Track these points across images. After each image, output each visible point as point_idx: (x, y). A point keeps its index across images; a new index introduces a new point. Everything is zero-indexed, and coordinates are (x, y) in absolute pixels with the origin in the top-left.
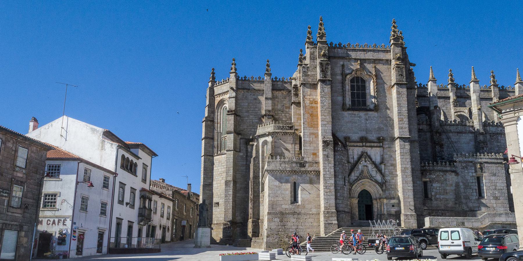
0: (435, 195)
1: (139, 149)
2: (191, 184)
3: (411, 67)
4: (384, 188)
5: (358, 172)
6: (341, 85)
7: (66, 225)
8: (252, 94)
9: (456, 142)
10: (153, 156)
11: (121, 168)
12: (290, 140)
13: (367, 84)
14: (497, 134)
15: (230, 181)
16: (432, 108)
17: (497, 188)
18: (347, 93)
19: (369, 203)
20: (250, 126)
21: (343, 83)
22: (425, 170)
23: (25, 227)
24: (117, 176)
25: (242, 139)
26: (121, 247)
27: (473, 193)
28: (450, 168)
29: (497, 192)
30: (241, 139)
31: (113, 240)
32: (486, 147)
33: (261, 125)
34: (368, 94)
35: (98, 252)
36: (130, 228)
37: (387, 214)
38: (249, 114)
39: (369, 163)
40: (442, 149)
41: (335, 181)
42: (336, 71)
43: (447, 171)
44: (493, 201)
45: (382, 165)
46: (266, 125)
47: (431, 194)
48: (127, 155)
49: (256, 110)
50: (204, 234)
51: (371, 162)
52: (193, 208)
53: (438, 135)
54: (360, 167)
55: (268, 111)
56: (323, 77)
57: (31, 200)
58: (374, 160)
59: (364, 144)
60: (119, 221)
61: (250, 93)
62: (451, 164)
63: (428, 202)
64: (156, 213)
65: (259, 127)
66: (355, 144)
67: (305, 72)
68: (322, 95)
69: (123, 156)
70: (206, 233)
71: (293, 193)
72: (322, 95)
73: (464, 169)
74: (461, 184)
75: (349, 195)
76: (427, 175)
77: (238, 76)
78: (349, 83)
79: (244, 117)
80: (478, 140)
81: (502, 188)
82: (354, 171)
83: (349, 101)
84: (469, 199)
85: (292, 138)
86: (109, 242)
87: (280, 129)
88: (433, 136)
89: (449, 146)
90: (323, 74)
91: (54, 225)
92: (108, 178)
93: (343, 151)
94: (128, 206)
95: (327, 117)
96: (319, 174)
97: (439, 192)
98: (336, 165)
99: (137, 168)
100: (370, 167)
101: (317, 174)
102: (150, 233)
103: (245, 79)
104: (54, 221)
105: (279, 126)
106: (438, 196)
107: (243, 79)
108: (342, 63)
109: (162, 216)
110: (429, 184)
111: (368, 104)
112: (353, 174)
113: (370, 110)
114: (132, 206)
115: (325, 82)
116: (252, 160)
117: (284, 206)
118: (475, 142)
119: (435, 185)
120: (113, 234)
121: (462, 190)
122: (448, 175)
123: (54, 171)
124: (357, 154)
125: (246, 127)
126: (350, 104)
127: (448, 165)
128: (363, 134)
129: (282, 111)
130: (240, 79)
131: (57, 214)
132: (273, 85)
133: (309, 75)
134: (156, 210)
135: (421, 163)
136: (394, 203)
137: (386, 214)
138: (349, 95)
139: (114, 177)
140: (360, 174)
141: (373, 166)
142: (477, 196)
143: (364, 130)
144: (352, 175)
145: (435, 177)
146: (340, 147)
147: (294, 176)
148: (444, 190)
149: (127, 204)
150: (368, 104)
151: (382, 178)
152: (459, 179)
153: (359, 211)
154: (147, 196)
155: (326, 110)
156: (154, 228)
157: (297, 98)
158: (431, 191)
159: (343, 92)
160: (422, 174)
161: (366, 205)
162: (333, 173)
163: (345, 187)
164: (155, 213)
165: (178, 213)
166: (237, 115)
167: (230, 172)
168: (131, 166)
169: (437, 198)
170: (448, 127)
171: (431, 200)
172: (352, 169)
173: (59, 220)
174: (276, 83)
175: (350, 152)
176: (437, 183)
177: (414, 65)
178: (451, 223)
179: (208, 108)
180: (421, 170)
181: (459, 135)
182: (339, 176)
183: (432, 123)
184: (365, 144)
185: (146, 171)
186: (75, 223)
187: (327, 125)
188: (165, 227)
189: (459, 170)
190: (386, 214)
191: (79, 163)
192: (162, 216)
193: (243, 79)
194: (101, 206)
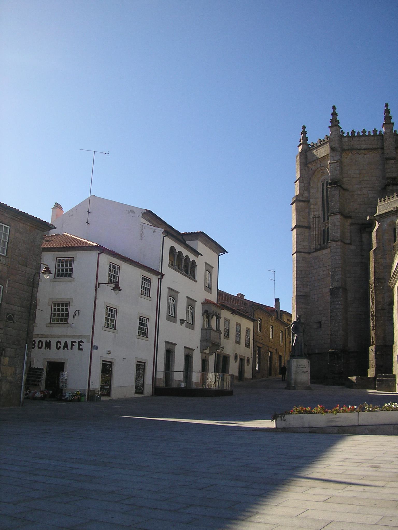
1: (198, 241)
2: (279, 299)
7: (82, 349)
10: (220, 254)
11: (169, 266)
15: (337, 288)
23: (9, 349)
24: (163, 278)
25: (353, 224)
26: (174, 385)
30: (352, 224)
31: (161, 376)
33: (383, 199)
35: (136, 393)
36: (188, 358)
38: (362, 187)
46: (391, 198)
48: (179, 248)
49: (373, 179)
50: (300, 369)
52: (284, 332)
57: (18, 308)
60: (170, 346)
61: (362, 155)
64: (229, 337)
65: (381, 201)
69: (172, 249)
70: (303, 366)
77: (342, 131)
86: (154, 379)
91: (66, 349)
92: (150, 280)
94: (184, 325)
99: (195, 269)
102: (221, 366)
103: (353, 135)
104: (66, 342)
107: (350, 135)
109: (238, 342)
114: (191, 325)
116: (372, 253)
120: (161, 365)
123: (64, 268)
130: (345, 135)
131: (69, 331)
134: (228, 333)
139: (159, 279)
149: (182, 321)
154: (213, 311)
156: (226, 359)
164: (227, 336)
165: (262, 339)
166: (344, 189)
167: (336, 274)
168: (186, 266)
173: (72, 342)
179: (299, 182)
185: (210, 274)
186: (96, 348)
188: (242, 358)
191: (99, 254)
192: (238, 342)
193: (350, 135)
194: (140, 323)
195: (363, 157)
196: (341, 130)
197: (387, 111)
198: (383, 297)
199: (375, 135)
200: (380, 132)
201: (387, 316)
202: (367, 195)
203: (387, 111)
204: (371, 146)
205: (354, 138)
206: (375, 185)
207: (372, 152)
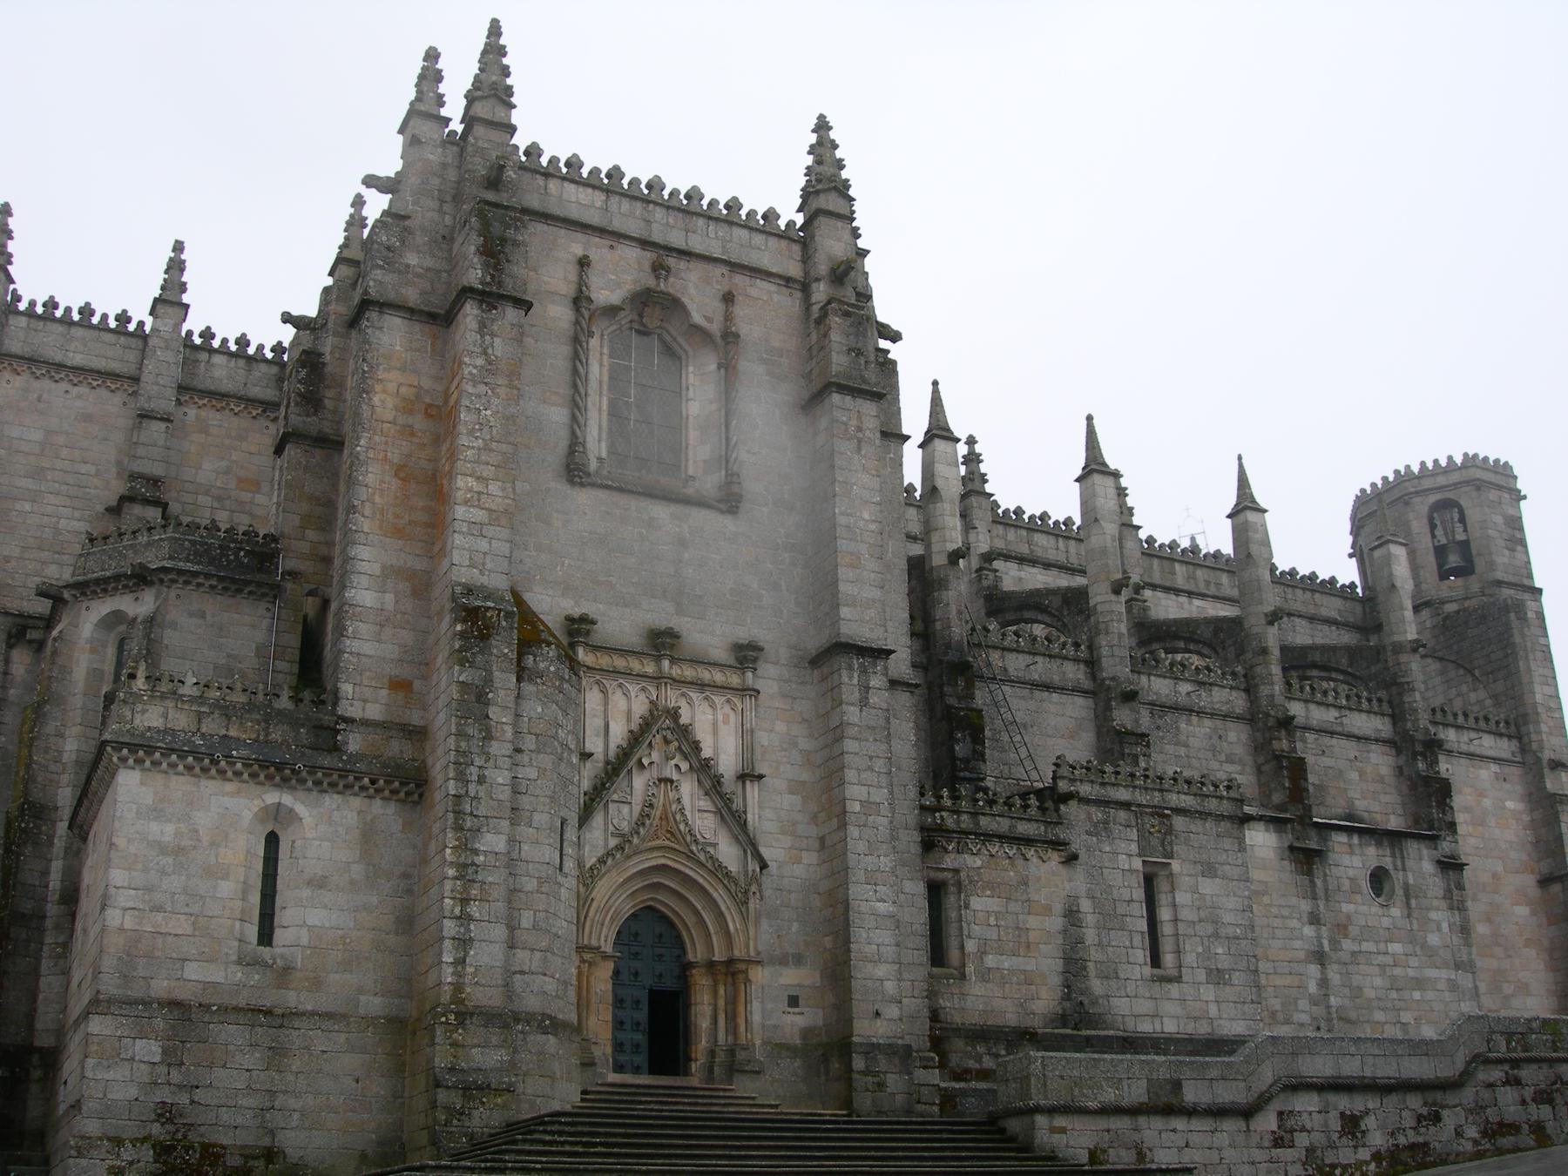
0: (982, 953)
3: (883, 344)
4: (753, 904)
5: (625, 809)
6: (565, 350)
8: (75, 391)
9: (1025, 726)
12: (254, 627)
13: (691, 376)
14: (1176, 708)
16: (938, 560)
17: (1223, 932)
18: (592, 399)
19: (670, 984)
20: (40, 549)
21: (576, 340)
22: (941, 829)
27: (1130, 950)
28: (1043, 828)
29: (1220, 951)
32: (1144, 756)
34: (691, 420)
37: (765, 1043)
38: (43, 488)
39: (684, 766)
40: (979, 748)
41: (512, 841)
42: (546, 279)
43: (1028, 841)
44: (1208, 993)
45: (748, 782)
47: (962, 948)
51: (696, 764)
53: (961, 683)
54: (639, 782)
55: (148, 480)
56: (488, 279)
58: (707, 752)
59: (666, 663)
61: (64, 386)
62: (1046, 805)
63: (949, 985)
66: (620, 663)
67: (388, 248)
68: (475, 371)
71: (255, 898)
72: (475, 371)
73: (1096, 835)
74: (1085, 905)
75: (575, 928)
76: (946, 850)
78: (601, 354)
79: (16, 499)
80: (1115, 723)
81: (1238, 931)
82: (606, 806)
83: (599, 441)
84: (1117, 978)
85: (269, 615)
87: (205, 559)
88: (941, 686)
89: (997, 741)
90: (486, 266)
93: (562, 679)
95: (494, 488)
96: (416, 797)
97: (995, 937)
98: (518, 750)
100: (688, 789)
101: (407, 794)
105: (202, 544)
106: (990, 961)
107: (39, 310)
108: (578, 250)
110: (951, 901)
111: (691, 472)
112: (598, 819)
113: (701, 503)
115: (496, 308)
117: (193, 971)
118: (1099, 735)
119: (977, 903)
121: (1090, 936)
122: (1035, 860)
124: (629, 713)
125: (17, 552)
126: (604, 455)
127: (1033, 812)
128: (661, 615)
129: (219, 499)
130: (22, 306)
132: (189, 364)
133: (408, 266)
135: (922, 795)
136: (798, 985)
137: (758, 1042)
138: (600, 410)
140: (640, 823)
141: (707, 783)
142: (1146, 964)
143: (665, 591)
144: (594, 825)
145: (979, 863)
146: (546, 661)
147: (272, 797)
148: (1018, 928)
150: (691, 472)
151: (745, 851)
152: (1076, 882)
153: (618, 1024)
155: (486, 448)
157: (314, 418)
158: (962, 935)
159: (575, 386)
160: (928, 846)
161: (651, 992)
162: (505, 794)
163: (560, 878)
169: (989, 969)
170: (995, 656)
171: (963, 977)
172: (595, 788)
174: (204, 356)
175: (593, 699)
176: (988, 892)
177: (895, 337)
178: (1125, 1083)
180: (922, 829)
181: (1037, 694)
182: (537, 817)
183: (938, 625)
184: (671, 668)
187: (490, 531)
189: (1078, 840)
190: (758, 1042)
193: (39, 310)
195: (67, 391)
196: (12, 287)
197: (176, 266)
198: (45, 873)
199: (121, 331)
200: (141, 324)
201: (51, 941)
202: (53, 520)
203: (176, 266)
204: (99, 364)
205: (49, 323)
206: (88, 490)
207: (99, 383)
